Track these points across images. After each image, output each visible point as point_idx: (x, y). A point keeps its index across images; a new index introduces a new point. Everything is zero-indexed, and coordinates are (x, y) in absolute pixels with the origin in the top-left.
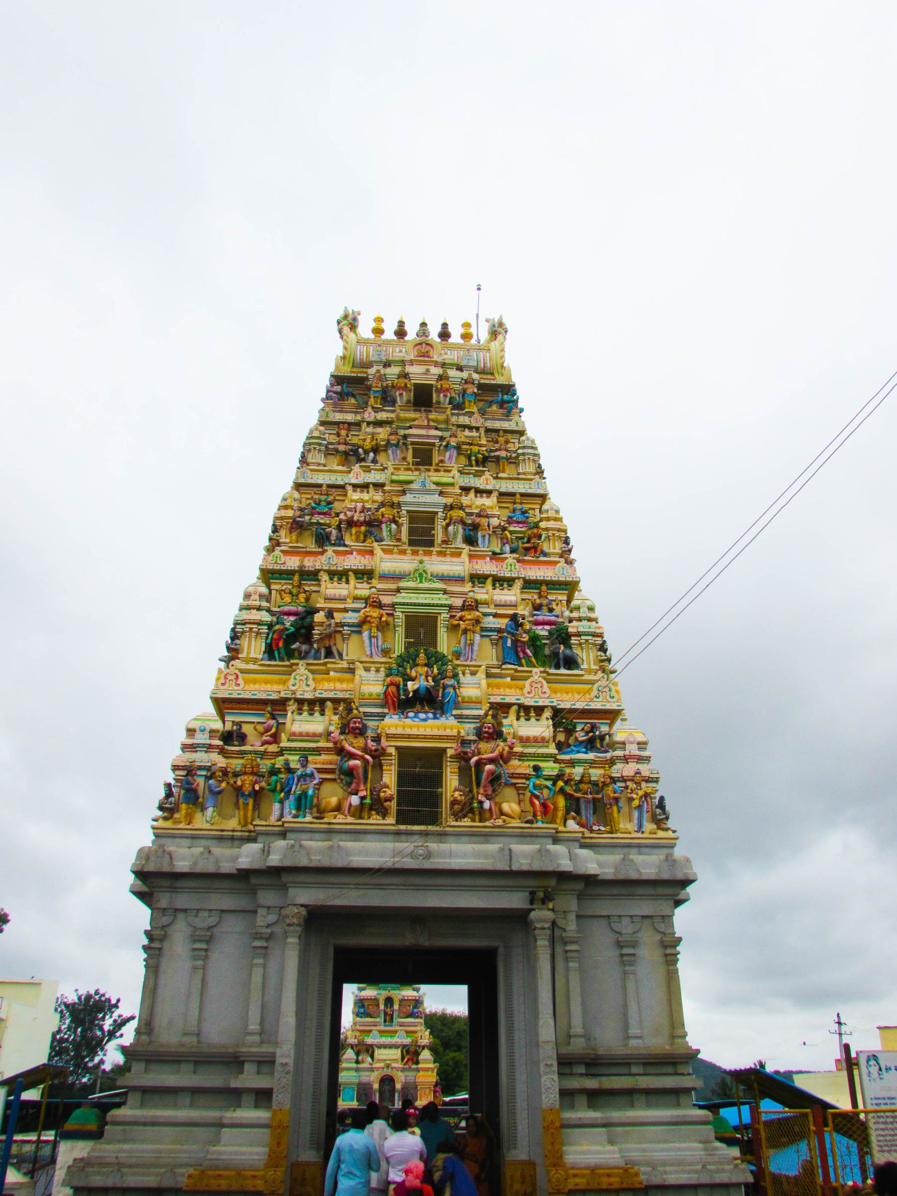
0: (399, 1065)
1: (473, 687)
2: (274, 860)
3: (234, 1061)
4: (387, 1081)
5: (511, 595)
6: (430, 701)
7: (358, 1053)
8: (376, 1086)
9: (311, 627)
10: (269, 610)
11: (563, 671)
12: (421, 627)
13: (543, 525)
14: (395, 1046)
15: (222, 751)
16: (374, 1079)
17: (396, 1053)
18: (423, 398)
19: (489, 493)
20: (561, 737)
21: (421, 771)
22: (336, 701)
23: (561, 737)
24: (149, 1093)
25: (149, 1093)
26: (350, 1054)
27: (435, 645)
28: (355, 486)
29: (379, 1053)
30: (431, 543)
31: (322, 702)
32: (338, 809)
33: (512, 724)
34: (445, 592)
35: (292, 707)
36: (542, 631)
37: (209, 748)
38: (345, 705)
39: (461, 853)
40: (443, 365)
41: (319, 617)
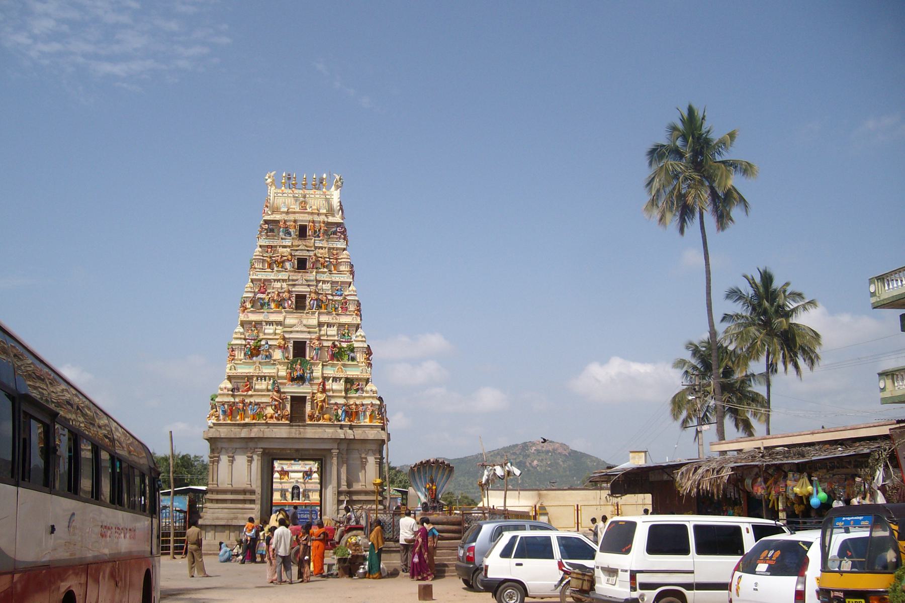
0: (302, 480)
1: (317, 372)
2: (253, 435)
3: (244, 492)
4: (295, 488)
5: (333, 331)
6: (301, 379)
7: (281, 475)
8: (290, 490)
9: (260, 347)
10: (245, 339)
11: (350, 362)
12: (300, 348)
13: (348, 298)
14: (300, 472)
15: (233, 396)
16: (289, 487)
17: (301, 475)
18: (302, 232)
19: (328, 282)
20: (349, 386)
21: (298, 401)
22: (270, 377)
23: (349, 386)
24: (212, 501)
25: (212, 501)
26: (276, 475)
27: (304, 356)
28: (275, 280)
29: (291, 475)
30: (304, 309)
31: (265, 377)
32: (272, 417)
33: (329, 385)
34: (309, 332)
35: (255, 379)
36: (344, 345)
37: (228, 395)
38: (274, 378)
39: (311, 433)
40: (312, 213)
41: (263, 342)
